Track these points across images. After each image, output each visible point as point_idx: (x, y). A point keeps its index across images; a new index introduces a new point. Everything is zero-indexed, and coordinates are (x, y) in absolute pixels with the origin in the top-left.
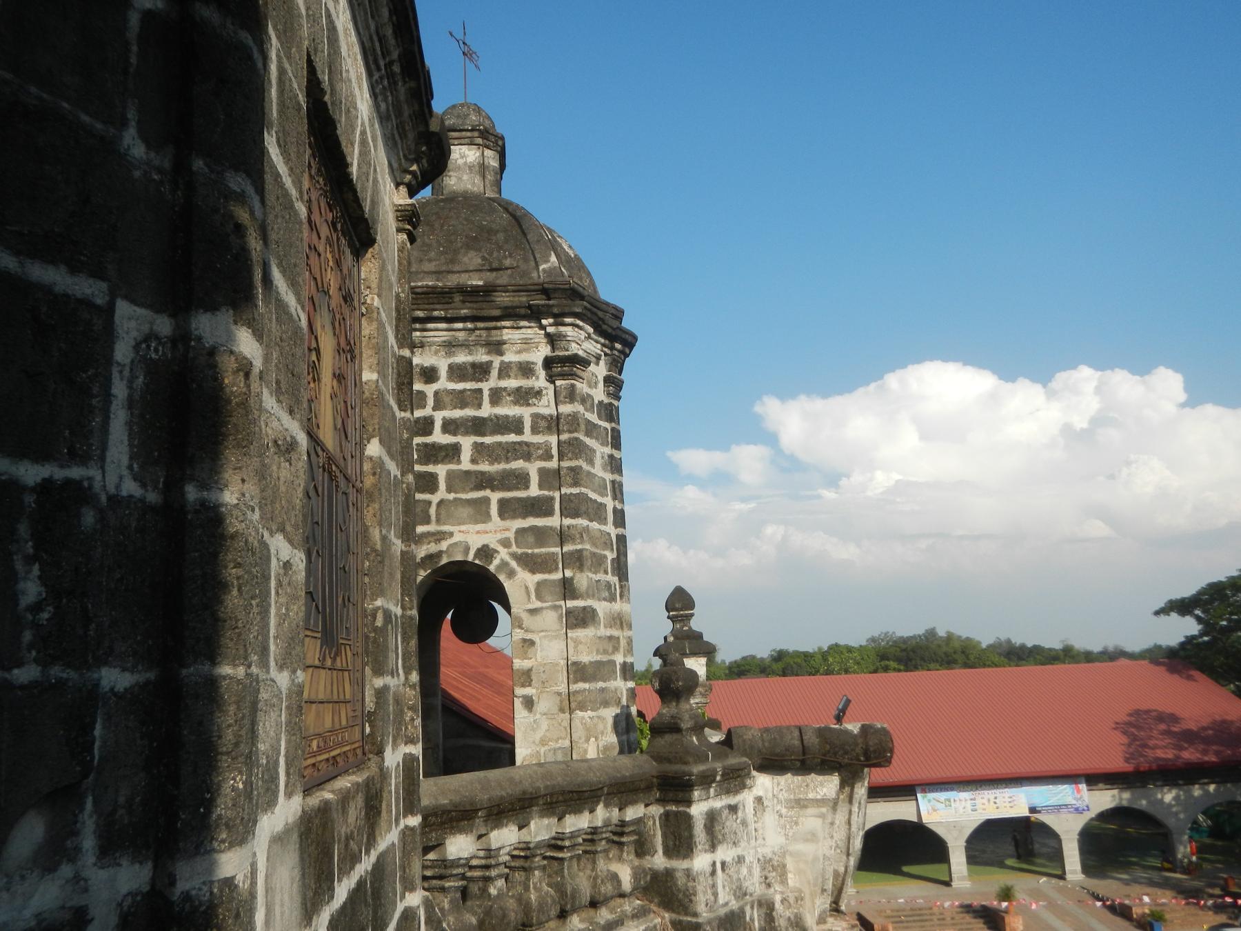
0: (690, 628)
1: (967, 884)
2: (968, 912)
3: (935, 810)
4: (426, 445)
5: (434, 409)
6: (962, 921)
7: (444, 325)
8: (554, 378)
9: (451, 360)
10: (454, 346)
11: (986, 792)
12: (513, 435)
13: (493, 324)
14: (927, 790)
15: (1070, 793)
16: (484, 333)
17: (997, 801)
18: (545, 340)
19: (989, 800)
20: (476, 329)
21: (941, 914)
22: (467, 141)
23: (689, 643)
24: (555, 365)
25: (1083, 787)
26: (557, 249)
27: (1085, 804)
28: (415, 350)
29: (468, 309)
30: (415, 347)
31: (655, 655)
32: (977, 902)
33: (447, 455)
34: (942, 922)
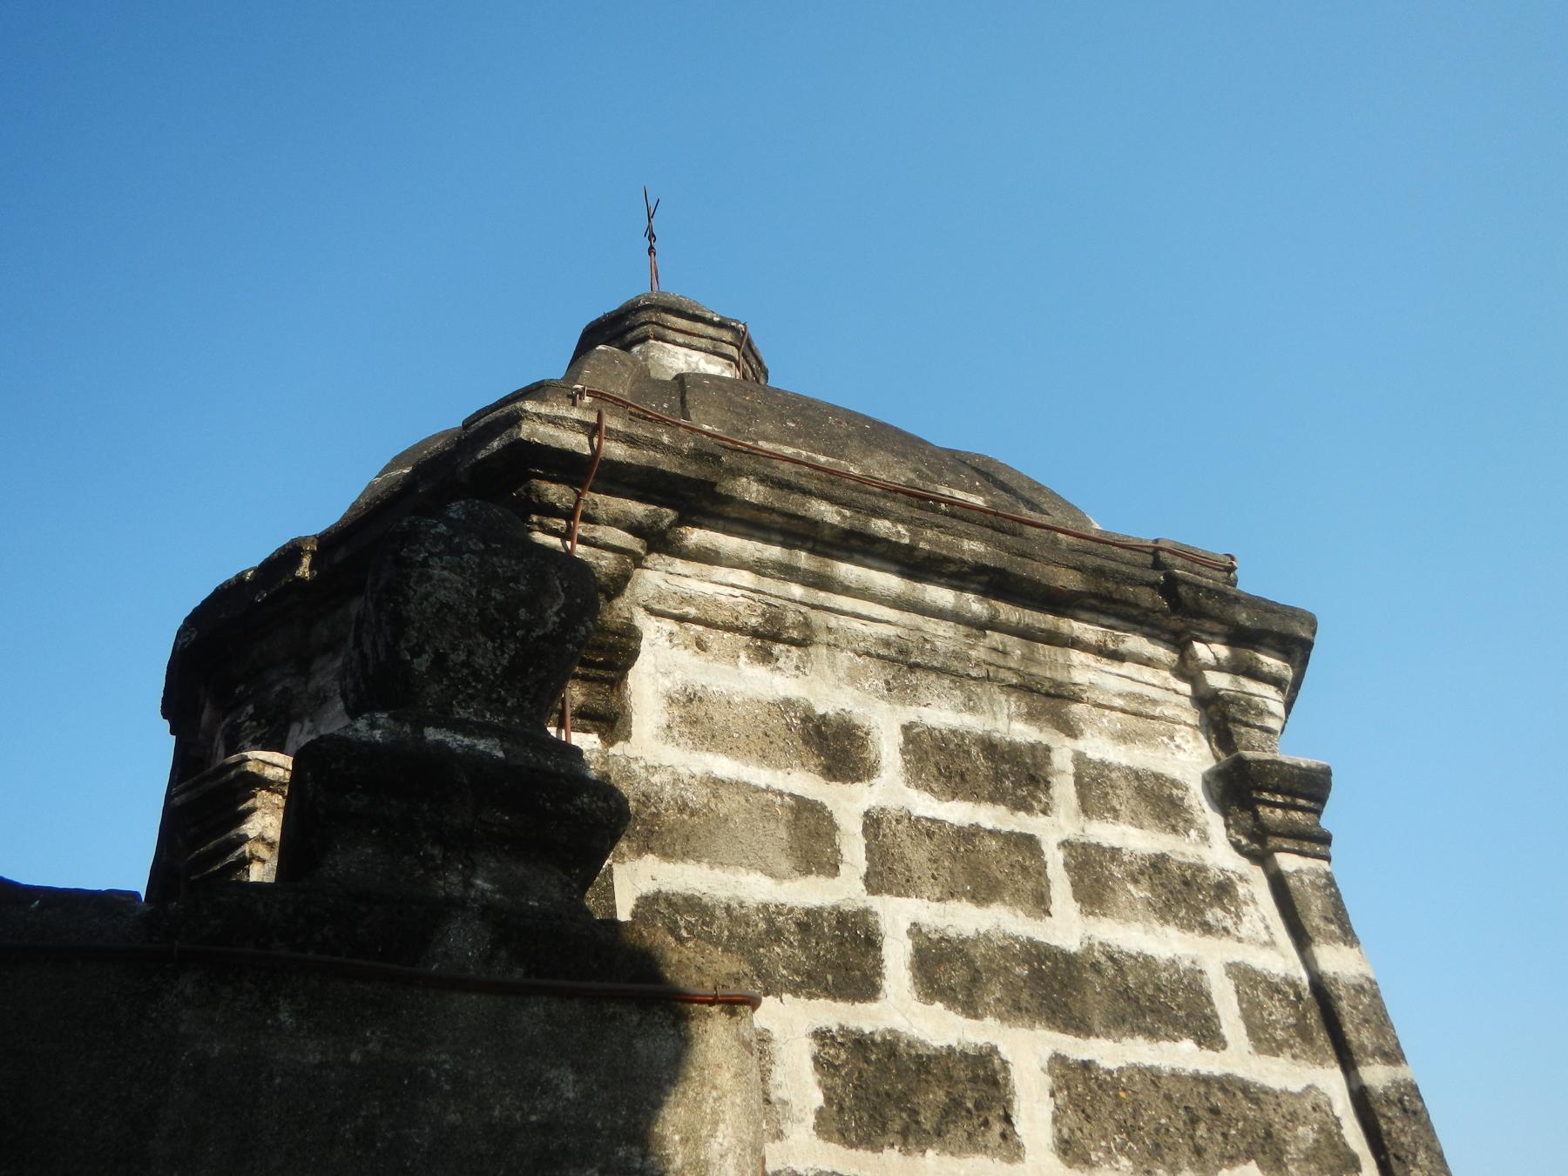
4: (860, 1043)
5: (876, 881)
7: (889, 582)
8: (1274, 842)
9: (910, 714)
10: (914, 667)
12: (1188, 1045)
13: (1045, 621)
16: (1016, 646)
18: (1191, 716)
20: (992, 624)
22: (704, 343)
24: (1266, 795)
26: (1025, 552)
28: (778, 649)
29: (987, 541)
30: (777, 638)
33: (952, 1110)
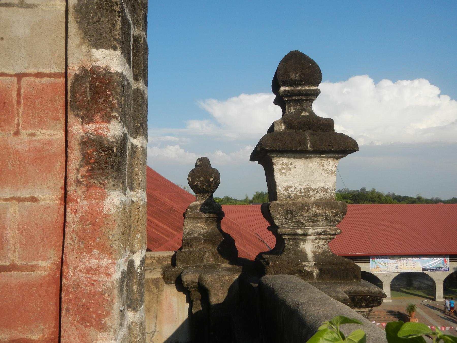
0: (312, 113)
1: (390, 301)
2: (392, 315)
3: (378, 268)
6: (388, 319)
11: (402, 260)
14: (375, 258)
15: (442, 263)
17: (407, 265)
19: (404, 264)
21: (379, 315)
23: (312, 134)
25: (448, 259)
27: (447, 268)
31: (253, 157)
32: (396, 309)
34: (380, 319)
